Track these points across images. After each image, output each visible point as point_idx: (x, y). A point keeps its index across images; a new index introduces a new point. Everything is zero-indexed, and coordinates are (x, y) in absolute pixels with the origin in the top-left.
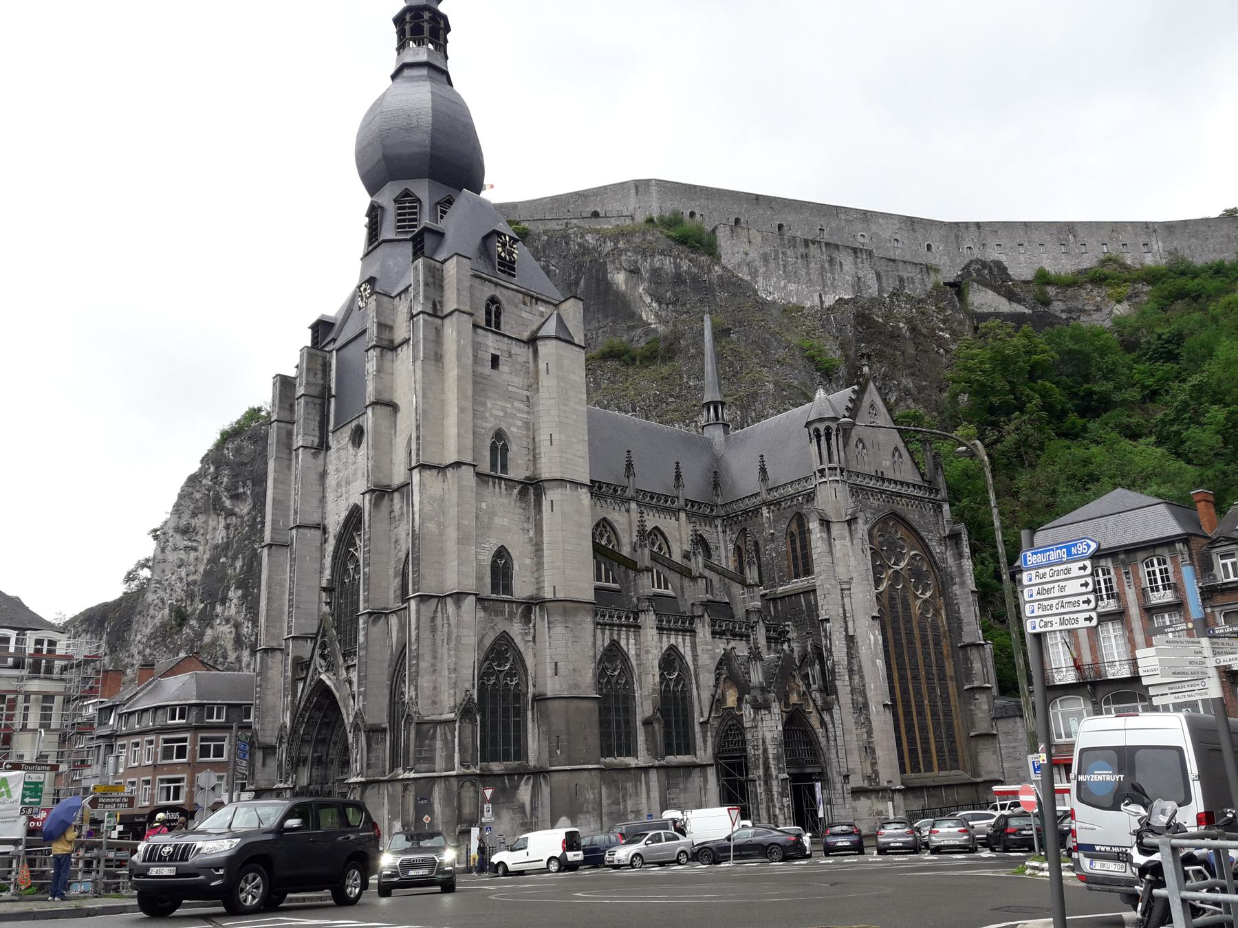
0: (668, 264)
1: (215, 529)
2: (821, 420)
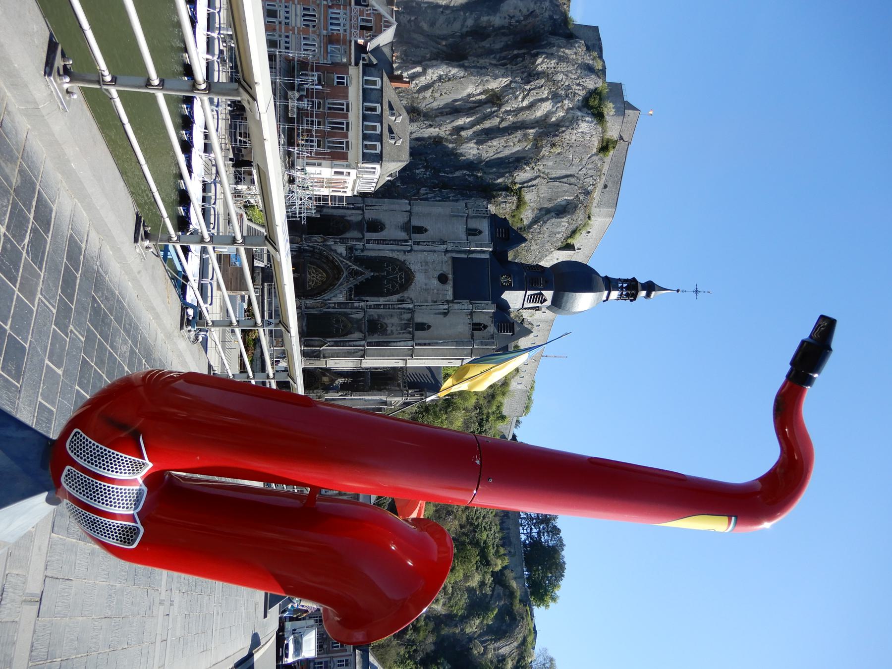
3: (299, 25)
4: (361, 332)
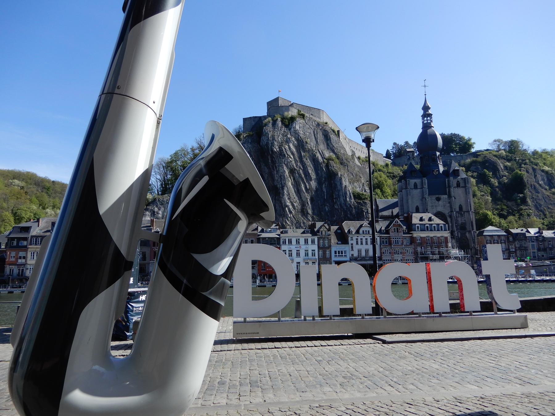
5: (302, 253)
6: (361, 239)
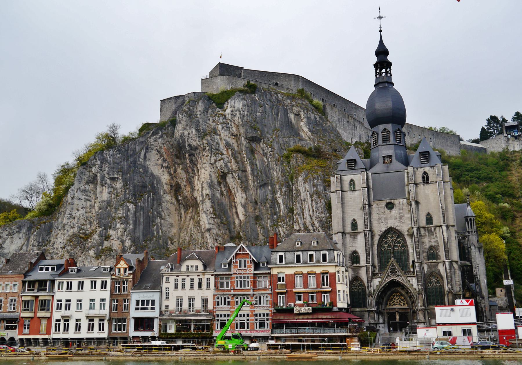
0: (312, 116)
1: (101, 192)
2: (472, 216)
3: (248, 308)
4: (437, 265)
5: (86, 304)
6: (184, 280)
